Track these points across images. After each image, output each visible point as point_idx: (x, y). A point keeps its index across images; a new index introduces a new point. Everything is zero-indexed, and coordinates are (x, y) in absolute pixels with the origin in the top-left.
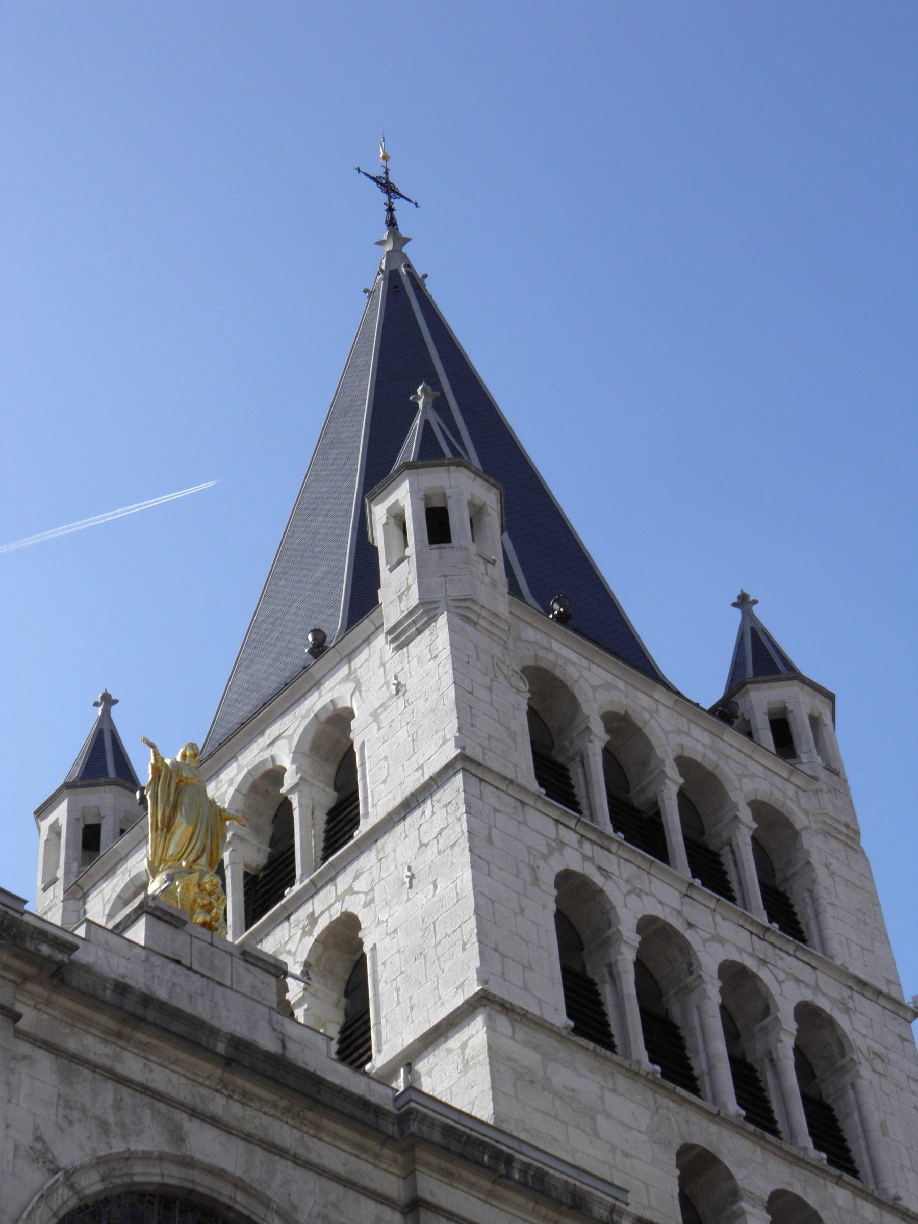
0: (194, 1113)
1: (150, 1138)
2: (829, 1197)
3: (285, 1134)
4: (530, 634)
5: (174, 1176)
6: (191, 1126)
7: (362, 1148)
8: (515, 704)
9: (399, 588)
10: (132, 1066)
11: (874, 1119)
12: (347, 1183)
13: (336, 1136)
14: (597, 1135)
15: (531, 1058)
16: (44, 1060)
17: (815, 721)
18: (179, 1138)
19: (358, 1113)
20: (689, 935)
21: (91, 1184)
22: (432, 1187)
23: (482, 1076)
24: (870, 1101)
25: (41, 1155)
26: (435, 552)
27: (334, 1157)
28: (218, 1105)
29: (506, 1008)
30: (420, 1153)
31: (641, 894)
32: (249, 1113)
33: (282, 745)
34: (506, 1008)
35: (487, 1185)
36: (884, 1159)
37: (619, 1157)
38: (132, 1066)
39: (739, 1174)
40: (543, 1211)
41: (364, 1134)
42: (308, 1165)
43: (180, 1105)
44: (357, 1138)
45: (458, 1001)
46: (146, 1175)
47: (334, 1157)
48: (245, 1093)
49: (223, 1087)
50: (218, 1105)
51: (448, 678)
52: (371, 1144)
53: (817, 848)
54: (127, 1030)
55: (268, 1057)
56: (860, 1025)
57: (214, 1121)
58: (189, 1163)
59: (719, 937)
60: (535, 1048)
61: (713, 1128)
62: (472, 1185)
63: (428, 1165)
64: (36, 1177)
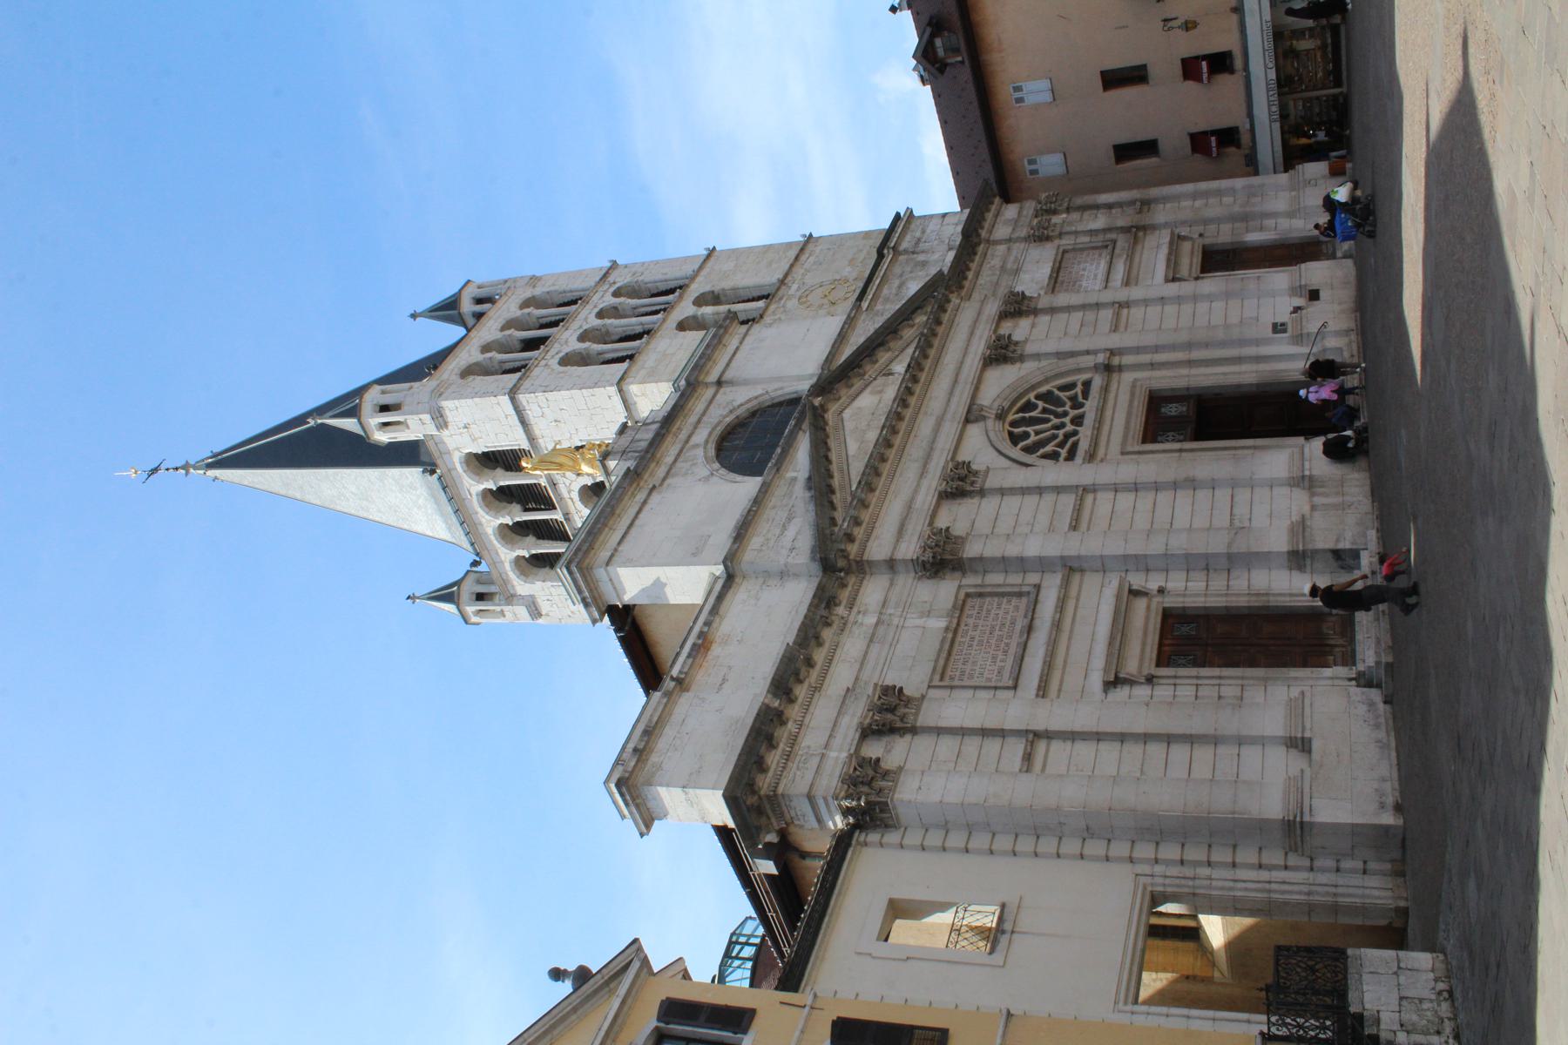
0: (687, 442)
1: (700, 452)
2: (696, 289)
3: (693, 419)
4: (445, 376)
6: (692, 442)
8: (478, 381)
9: (415, 428)
11: (659, 277)
15: (643, 372)
16: (668, 481)
17: (479, 287)
18: (697, 446)
21: (717, 465)
22: (713, 377)
23: (651, 387)
24: (652, 278)
25: (706, 479)
26: (405, 408)
27: (700, 407)
28: (683, 436)
29: (622, 379)
31: (567, 340)
33: (474, 486)
36: (678, 274)
38: (669, 459)
42: (704, 414)
45: (617, 399)
46: (712, 452)
47: (700, 407)
50: (683, 436)
51: (469, 401)
53: (538, 291)
55: (662, 427)
56: (620, 279)
57: (690, 437)
58: (707, 442)
59: (586, 318)
64: (715, 479)
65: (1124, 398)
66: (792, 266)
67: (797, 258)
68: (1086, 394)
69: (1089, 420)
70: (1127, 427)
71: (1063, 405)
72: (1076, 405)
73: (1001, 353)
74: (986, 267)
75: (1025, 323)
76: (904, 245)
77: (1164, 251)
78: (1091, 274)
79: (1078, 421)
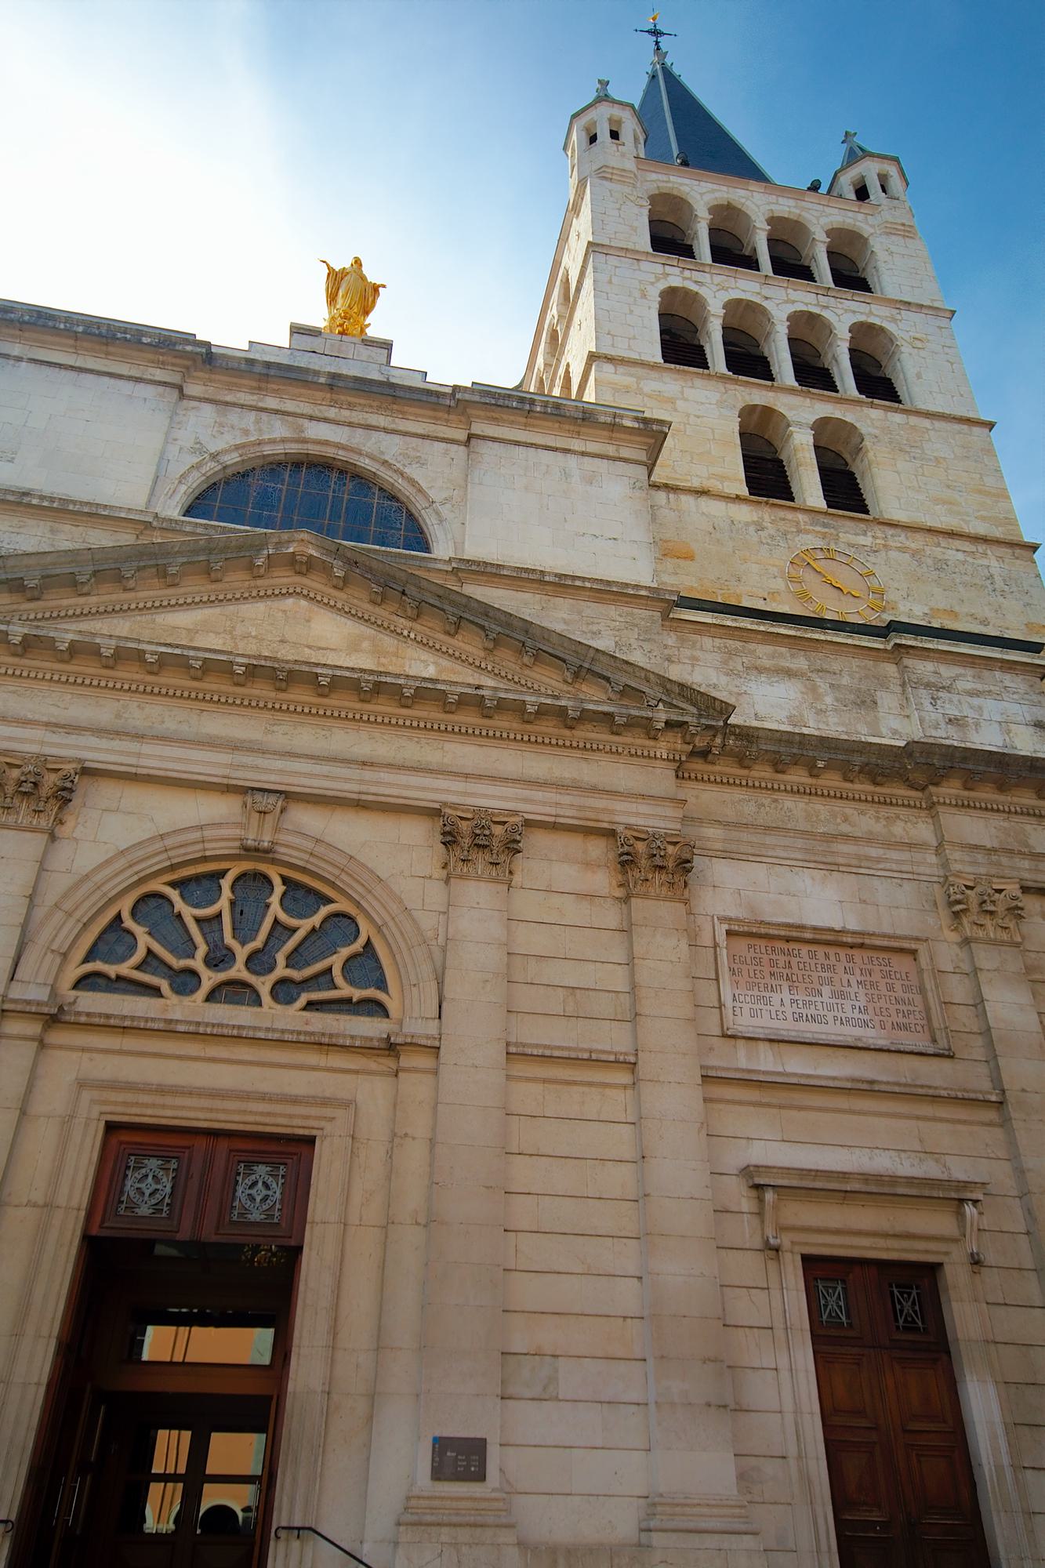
5: (294, 448)
7: (435, 418)
10: (271, 402)
12: (423, 437)
13: (416, 415)
14: (676, 410)
15: (629, 381)
19: (424, 398)
20: (765, 304)
29: (610, 359)
30: (470, 411)
32: (354, 414)
34: (610, 359)
35: (523, 420)
37: (692, 418)
39: (790, 415)
40: (567, 427)
41: (434, 410)
43: (302, 416)
44: (431, 413)
48: (349, 404)
49: (334, 403)
52: (440, 414)
54: (263, 385)
58: (305, 441)
60: (632, 375)
61: (771, 394)
62: (512, 422)
63: (478, 417)
65: (297, 1083)
66: (930, 531)
67: (952, 534)
68: (311, 1006)
69: (240, 1015)
70: (162, 1090)
71: (292, 961)
72: (284, 991)
73: (477, 843)
74: (849, 809)
75: (603, 881)
76: (924, 668)
77: (906, 1167)
78: (839, 1009)
79: (235, 992)
